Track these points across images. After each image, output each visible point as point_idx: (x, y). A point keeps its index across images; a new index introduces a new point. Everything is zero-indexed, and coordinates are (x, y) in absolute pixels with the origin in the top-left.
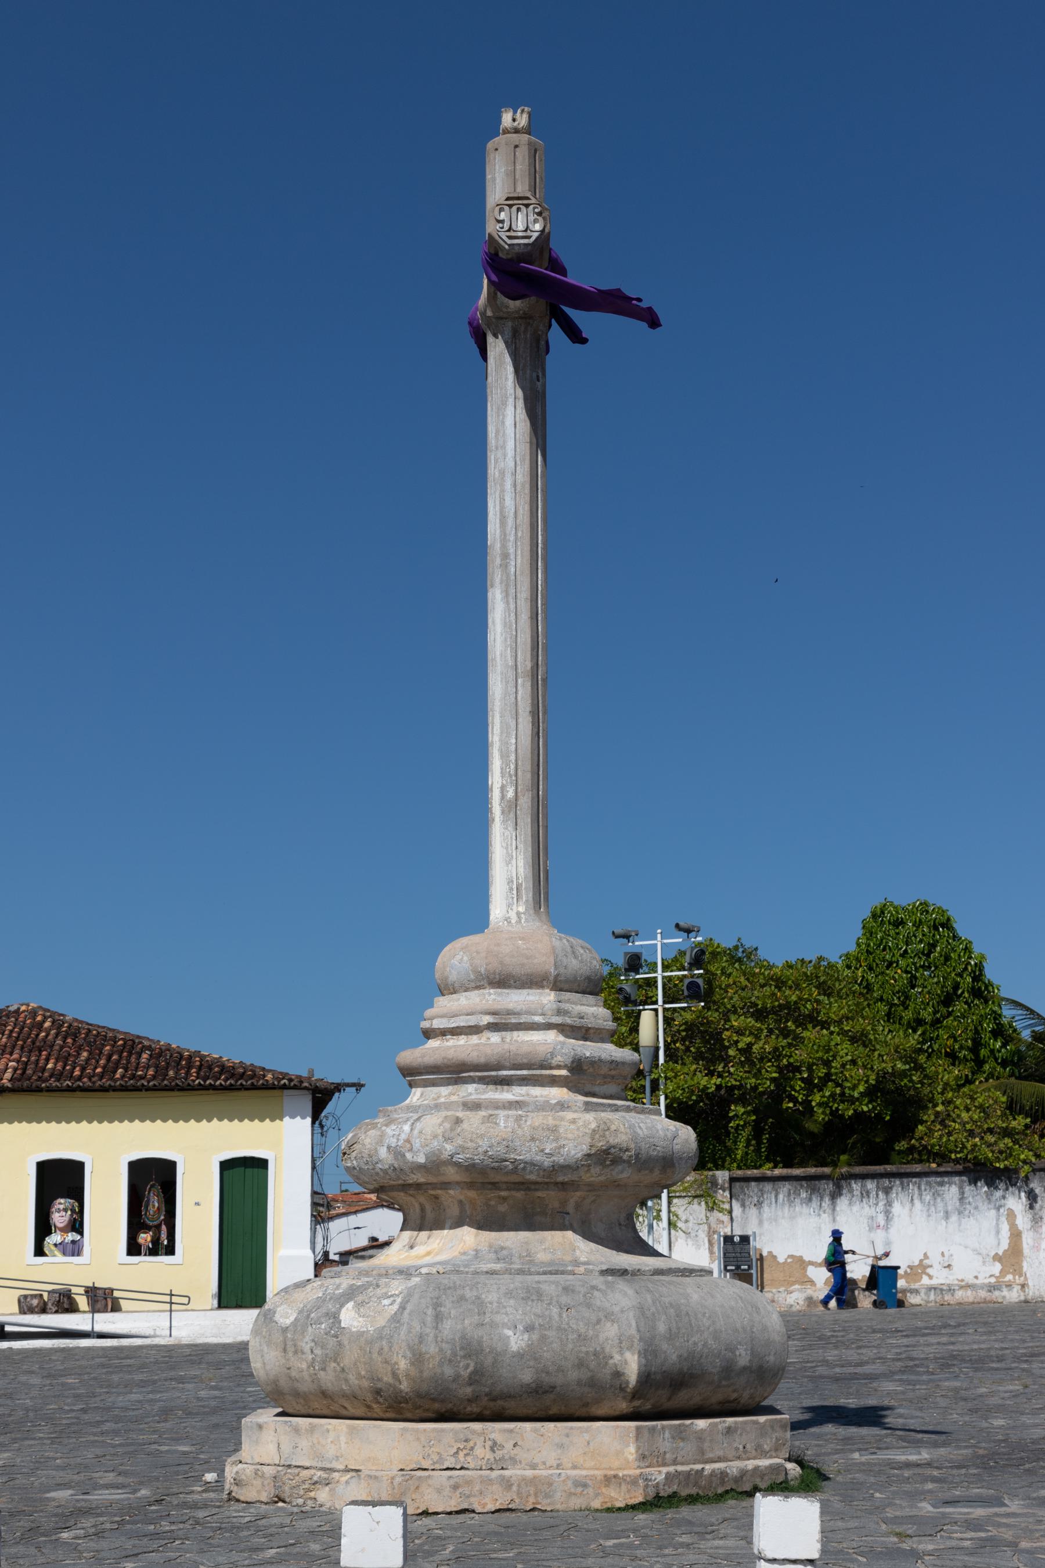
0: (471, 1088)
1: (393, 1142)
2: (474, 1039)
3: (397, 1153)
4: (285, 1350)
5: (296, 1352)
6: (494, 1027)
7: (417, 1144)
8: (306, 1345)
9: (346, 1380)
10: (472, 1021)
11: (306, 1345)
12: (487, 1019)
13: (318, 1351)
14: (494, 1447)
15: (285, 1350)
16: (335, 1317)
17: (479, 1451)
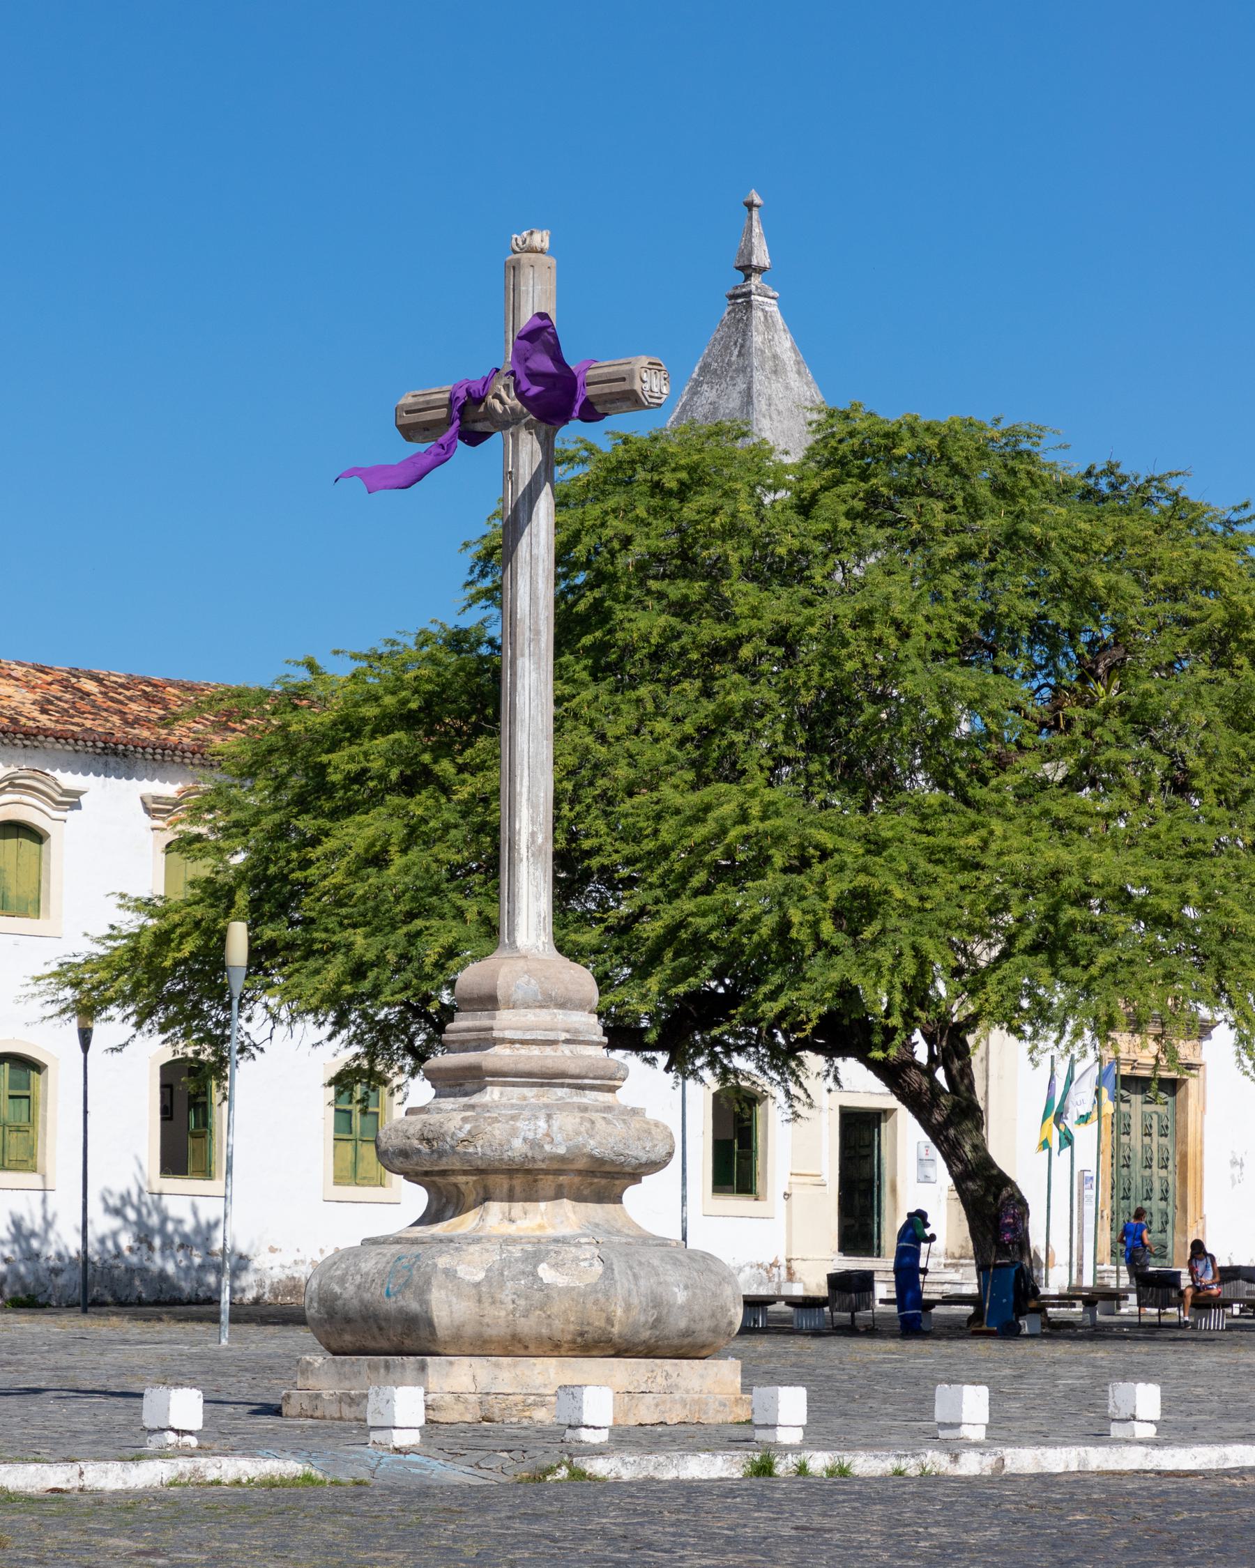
0: (561, 1092)
1: (531, 1135)
2: (548, 1050)
3: (534, 1144)
4: (480, 1301)
5: (493, 1303)
6: (567, 1041)
7: (558, 1138)
8: (506, 1296)
9: (550, 1325)
10: (551, 1036)
11: (506, 1296)
12: (564, 1036)
13: (522, 1302)
14: (667, 1376)
15: (480, 1301)
16: (534, 1274)
17: (660, 1380)
